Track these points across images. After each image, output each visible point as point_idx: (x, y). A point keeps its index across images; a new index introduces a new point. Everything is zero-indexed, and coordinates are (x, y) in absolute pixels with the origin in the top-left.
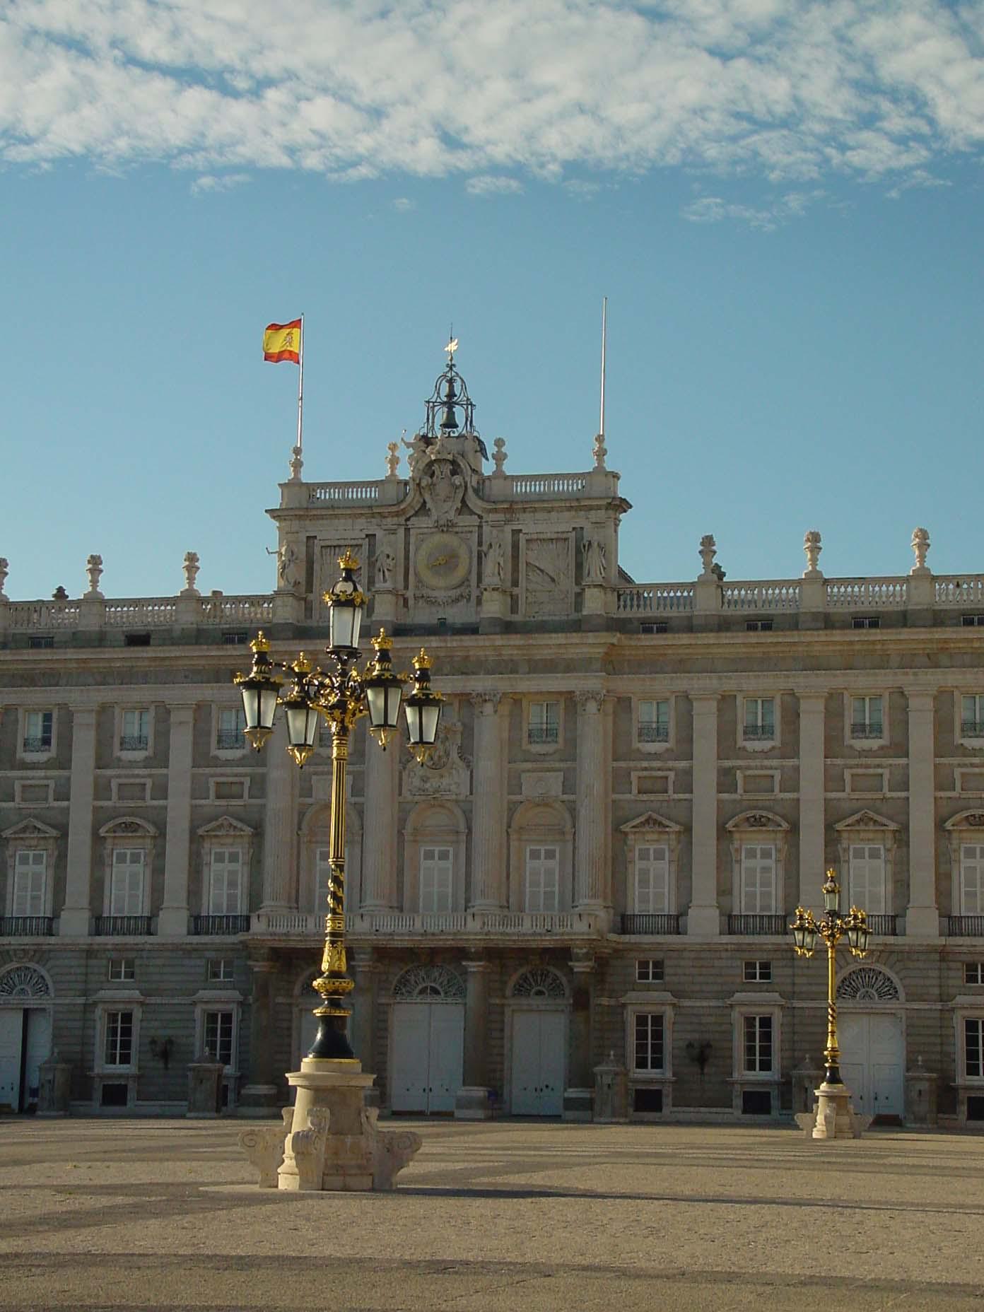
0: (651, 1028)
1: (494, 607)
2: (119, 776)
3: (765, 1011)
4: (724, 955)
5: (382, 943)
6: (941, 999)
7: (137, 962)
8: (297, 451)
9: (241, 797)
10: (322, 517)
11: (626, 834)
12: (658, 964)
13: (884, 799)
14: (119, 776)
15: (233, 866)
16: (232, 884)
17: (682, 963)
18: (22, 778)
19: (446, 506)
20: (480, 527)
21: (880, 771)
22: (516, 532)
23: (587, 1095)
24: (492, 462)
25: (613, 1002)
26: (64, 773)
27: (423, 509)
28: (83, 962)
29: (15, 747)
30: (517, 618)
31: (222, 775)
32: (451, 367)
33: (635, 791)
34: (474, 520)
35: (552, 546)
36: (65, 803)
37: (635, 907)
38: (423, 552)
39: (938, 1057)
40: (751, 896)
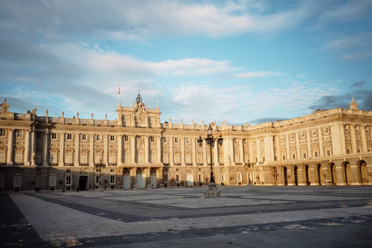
6: (197, 172)
9: (114, 147)
10: (125, 111)
12: (167, 169)
16: (113, 159)
20: (144, 115)
32: (139, 94)
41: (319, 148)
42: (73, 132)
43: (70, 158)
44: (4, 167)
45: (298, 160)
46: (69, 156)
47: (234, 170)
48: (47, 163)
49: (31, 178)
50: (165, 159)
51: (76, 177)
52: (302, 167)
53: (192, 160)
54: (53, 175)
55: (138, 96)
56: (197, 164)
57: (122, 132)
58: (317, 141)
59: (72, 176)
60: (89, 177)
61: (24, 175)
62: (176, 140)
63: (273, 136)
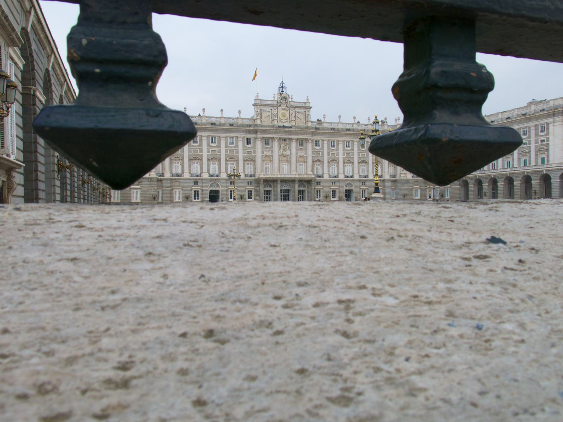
1: (293, 124)
3: (335, 189)
8: (258, 94)
9: (251, 153)
10: (263, 106)
12: (319, 182)
13: (351, 157)
16: (251, 169)
19: (284, 106)
27: (280, 106)
29: (209, 143)
30: (296, 126)
32: (282, 81)
35: (301, 114)
38: (281, 113)
40: (332, 172)
41: (530, 155)
43: (197, 167)
45: (499, 171)
46: (196, 165)
48: (170, 173)
50: (317, 169)
52: (503, 180)
53: (353, 170)
57: (261, 133)
58: (527, 144)
59: (201, 189)
60: (220, 191)
62: (331, 144)
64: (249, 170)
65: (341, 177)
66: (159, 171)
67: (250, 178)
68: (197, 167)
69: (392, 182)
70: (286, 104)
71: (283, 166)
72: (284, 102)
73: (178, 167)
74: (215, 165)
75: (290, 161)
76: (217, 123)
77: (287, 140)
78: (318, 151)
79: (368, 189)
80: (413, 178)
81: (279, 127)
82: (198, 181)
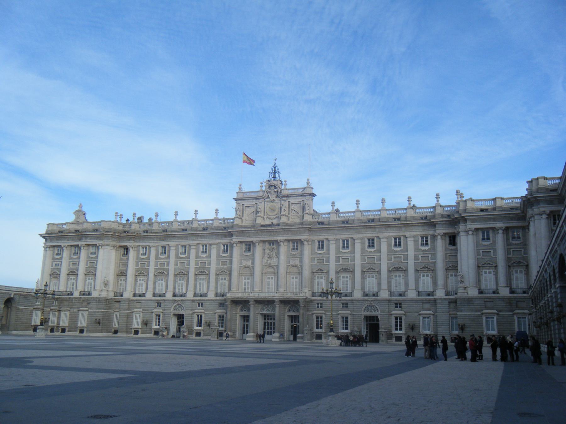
0: (319, 319)
1: (284, 219)
2: (200, 260)
4: (337, 302)
5: (256, 299)
7: (203, 303)
8: (240, 185)
11: (314, 273)
12: (321, 304)
13: (375, 263)
14: (200, 260)
15: (225, 281)
17: (327, 304)
18: (179, 261)
19: (273, 196)
21: (374, 257)
22: (289, 202)
23: (303, 336)
24: (284, 186)
25: (310, 313)
26: (188, 260)
28: (191, 303)
31: (223, 260)
32: (275, 164)
33: (316, 263)
34: (280, 199)
36: (188, 267)
37: (316, 291)
39: (388, 326)
42: (167, 243)
44: (70, 298)
46: (161, 282)
47: (473, 307)
49: (97, 314)
50: (318, 284)
51: (166, 315)
53: (379, 284)
54: (137, 312)
55: (274, 168)
56: (391, 294)
57: (237, 236)
60: (184, 316)
61: (90, 310)
63: (548, 212)
64: (223, 287)
65: (358, 295)
66: (123, 291)
67: (221, 298)
68: (162, 284)
69: (449, 302)
70: (276, 194)
71: (269, 280)
72: (272, 192)
73: (142, 284)
74: (182, 281)
75: (278, 273)
76: (188, 228)
77: (275, 243)
78: (321, 256)
79: (405, 315)
80: (480, 295)
81: (262, 226)
82: (160, 302)
